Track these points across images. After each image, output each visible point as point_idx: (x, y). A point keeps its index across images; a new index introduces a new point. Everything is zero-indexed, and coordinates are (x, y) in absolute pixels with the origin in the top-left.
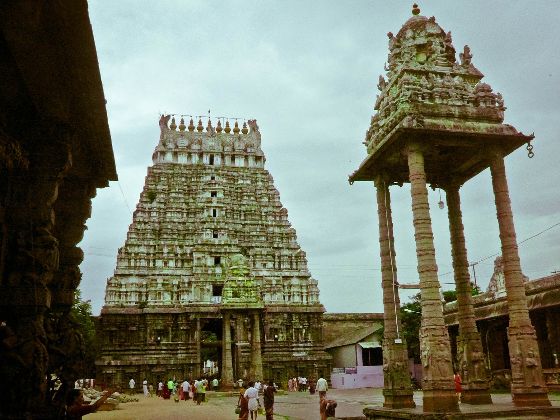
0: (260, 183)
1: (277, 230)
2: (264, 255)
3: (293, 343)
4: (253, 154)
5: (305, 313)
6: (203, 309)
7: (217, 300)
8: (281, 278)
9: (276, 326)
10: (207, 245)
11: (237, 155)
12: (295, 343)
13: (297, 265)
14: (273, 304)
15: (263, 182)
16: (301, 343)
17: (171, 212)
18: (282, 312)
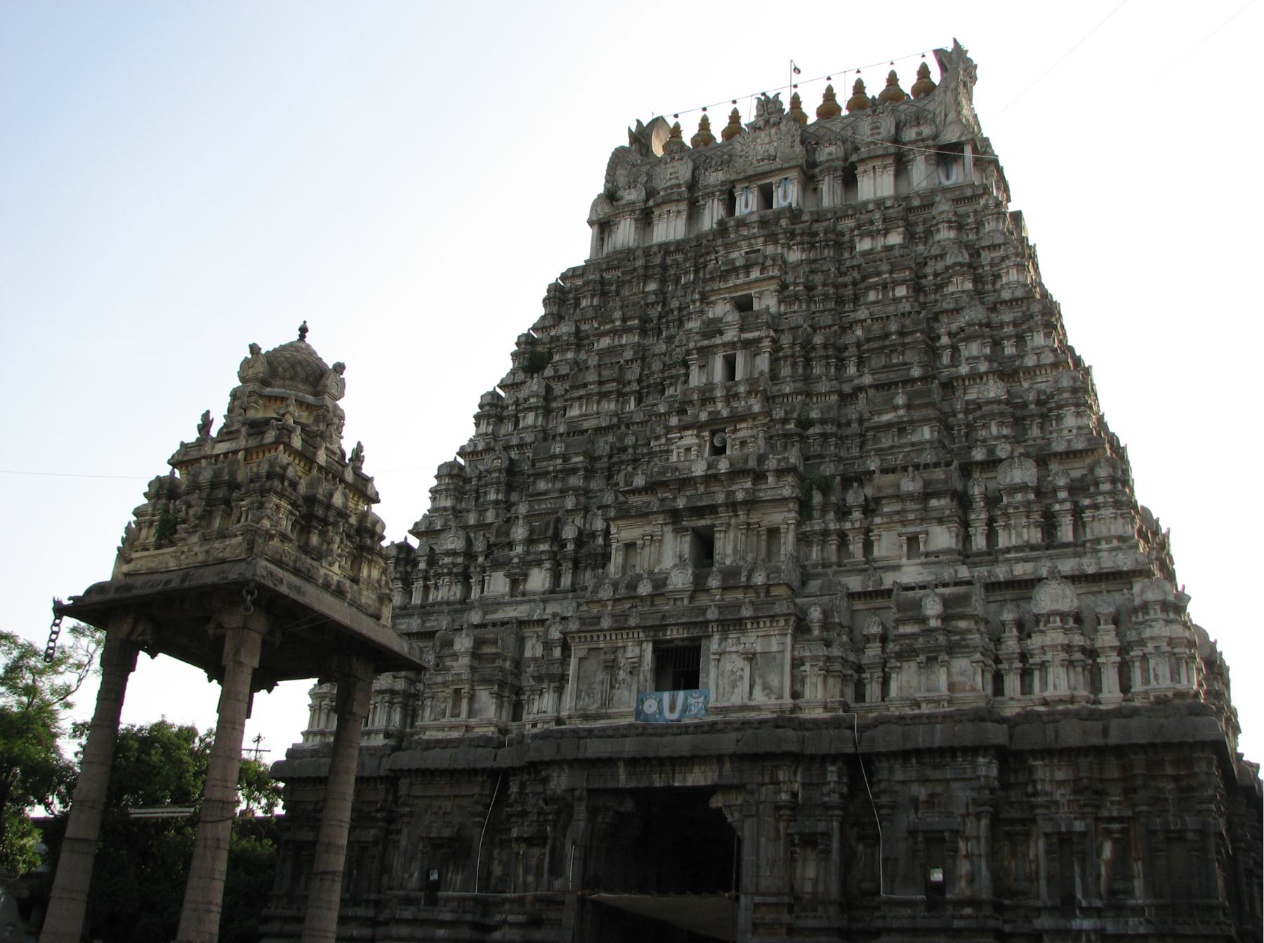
0: (945, 234)
1: (994, 389)
2: (910, 496)
3: (1039, 911)
4: (930, 142)
5: (1100, 752)
6: (595, 749)
7: (669, 707)
9: (934, 820)
10: (664, 484)
11: (863, 161)
12: (1051, 910)
13: (1079, 524)
14: (925, 709)
15: (960, 226)
16: (1088, 912)
17: (580, 398)
18: (965, 750)
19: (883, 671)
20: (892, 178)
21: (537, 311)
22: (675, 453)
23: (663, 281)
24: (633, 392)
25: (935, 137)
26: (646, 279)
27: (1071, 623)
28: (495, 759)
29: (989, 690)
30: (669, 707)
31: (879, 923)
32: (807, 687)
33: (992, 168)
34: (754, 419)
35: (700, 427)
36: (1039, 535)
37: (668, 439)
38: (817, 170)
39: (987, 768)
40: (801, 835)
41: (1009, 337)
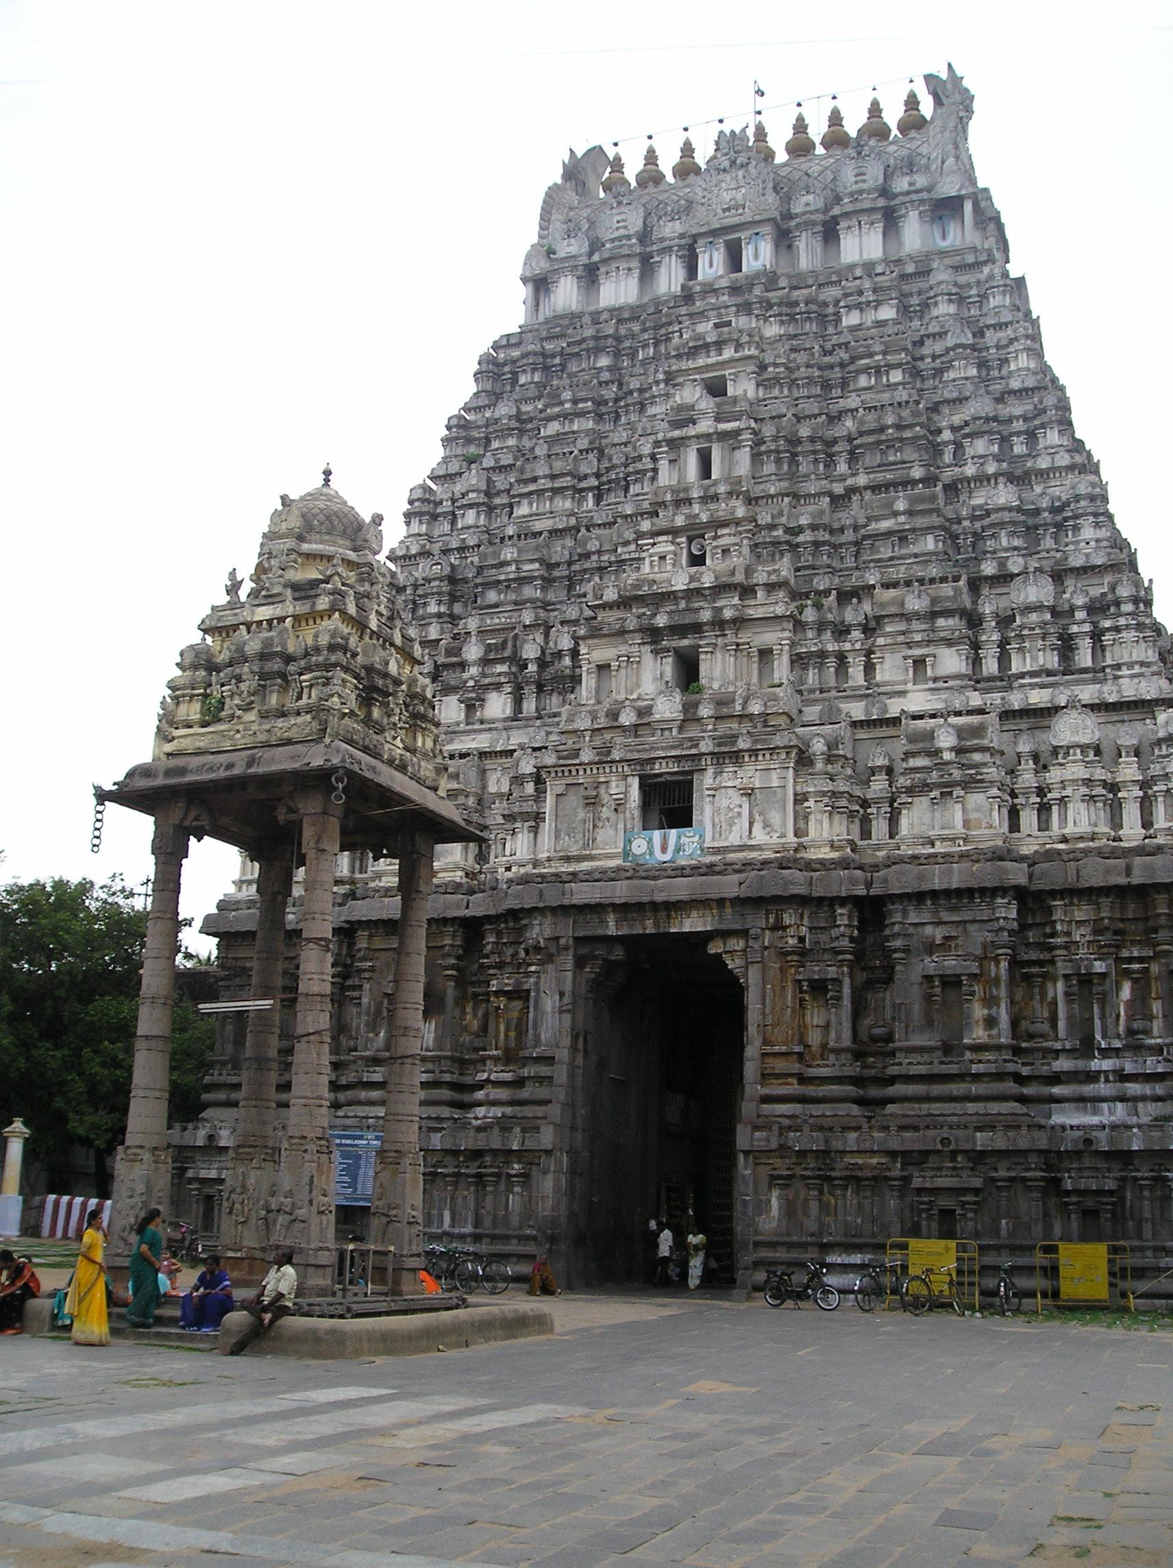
0: (944, 309)
1: (1004, 495)
2: (917, 616)
3: (1057, 1053)
4: (925, 195)
5: (1121, 892)
6: (582, 894)
7: (661, 846)
8: (992, 718)
9: (951, 964)
10: (640, 600)
11: (846, 215)
12: (1070, 1052)
13: (1098, 646)
14: (940, 848)
15: (960, 300)
17: (531, 493)
18: (983, 891)
19: (891, 805)
20: (881, 236)
21: (466, 389)
22: (647, 561)
23: (617, 354)
24: (590, 489)
25: (929, 189)
26: (598, 351)
27: (1091, 757)
28: (467, 907)
29: (1005, 828)
30: (661, 846)
31: (894, 1070)
32: (812, 825)
33: (992, 226)
34: (737, 524)
35: (674, 532)
36: (1056, 659)
37: (638, 545)
38: (793, 223)
39: (1007, 911)
40: (810, 981)
41: (1018, 434)
